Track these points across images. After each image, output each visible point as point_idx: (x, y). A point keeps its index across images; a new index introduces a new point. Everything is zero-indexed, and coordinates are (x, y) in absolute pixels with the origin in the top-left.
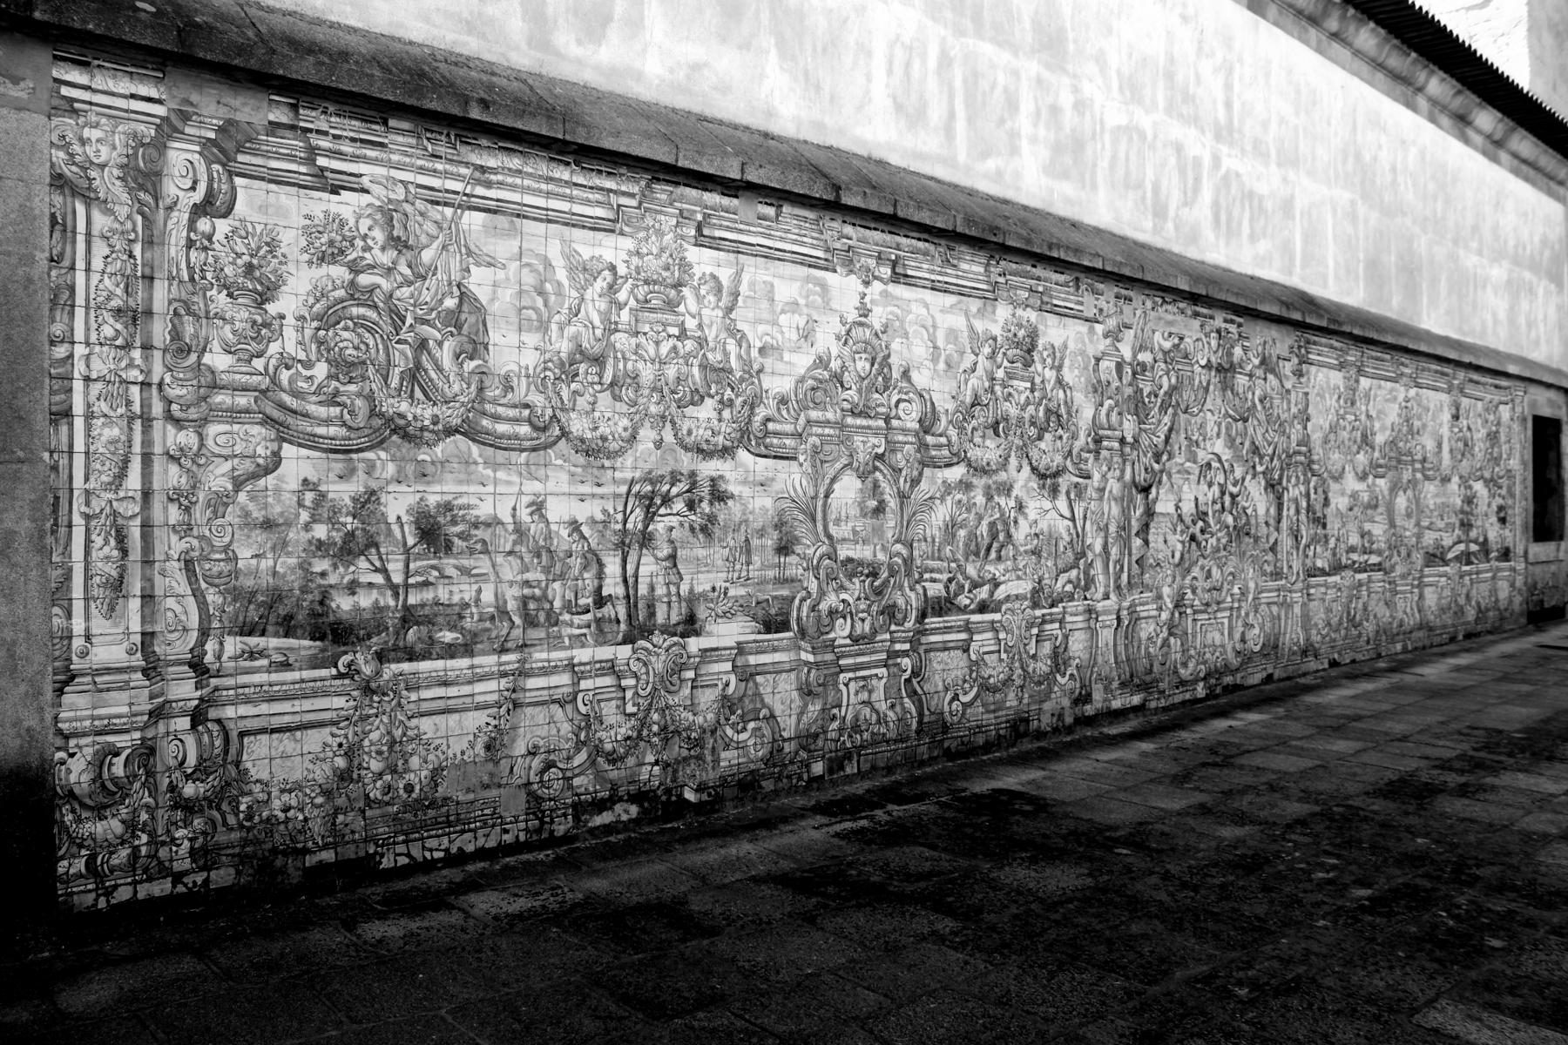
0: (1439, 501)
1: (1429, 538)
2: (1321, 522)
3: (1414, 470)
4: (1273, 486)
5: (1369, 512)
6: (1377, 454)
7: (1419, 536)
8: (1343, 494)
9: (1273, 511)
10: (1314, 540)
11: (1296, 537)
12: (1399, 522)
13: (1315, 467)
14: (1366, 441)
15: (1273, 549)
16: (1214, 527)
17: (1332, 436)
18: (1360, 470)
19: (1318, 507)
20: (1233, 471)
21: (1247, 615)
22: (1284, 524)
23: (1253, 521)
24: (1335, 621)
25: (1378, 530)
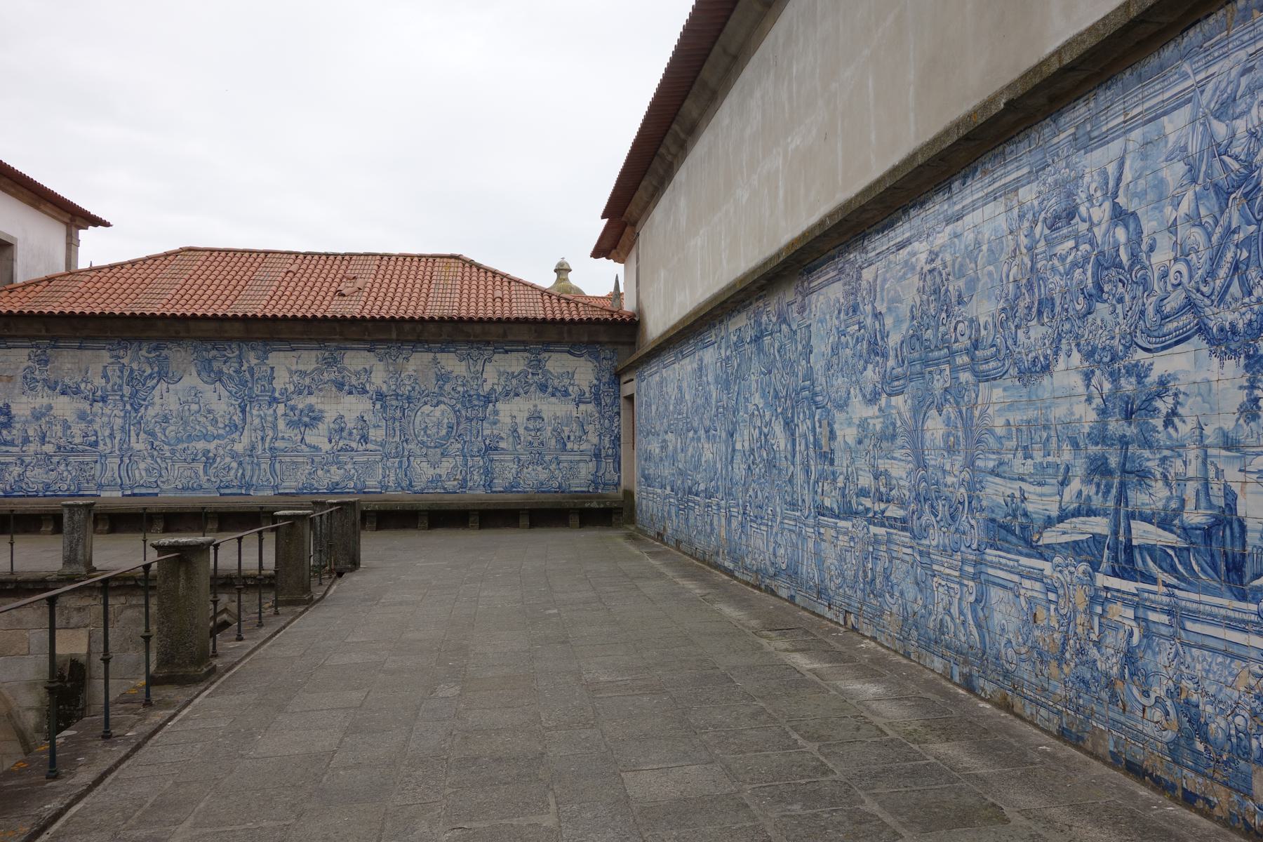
0: (1016, 417)
1: (996, 492)
2: (828, 457)
3: (955, 370)
4: (789, 425)
5: (885, 445)
6: (891, 362)
7: (973, 487)
8: (850, 424)
9: (789, 447)
10: (822, 477)
11: (807, 472)
12: (932, 459)
13: (819, 399)
14: (876, 349)
15: (790, 481)
16: (758, 460)
17: (835, 360)
18: (869, 388)
19: (824, 442)
20: (764, 416)
21: (776, 534)
22: (798, 458)
23: (778, 456)
24: (849, 574)
25: (899, 469)
